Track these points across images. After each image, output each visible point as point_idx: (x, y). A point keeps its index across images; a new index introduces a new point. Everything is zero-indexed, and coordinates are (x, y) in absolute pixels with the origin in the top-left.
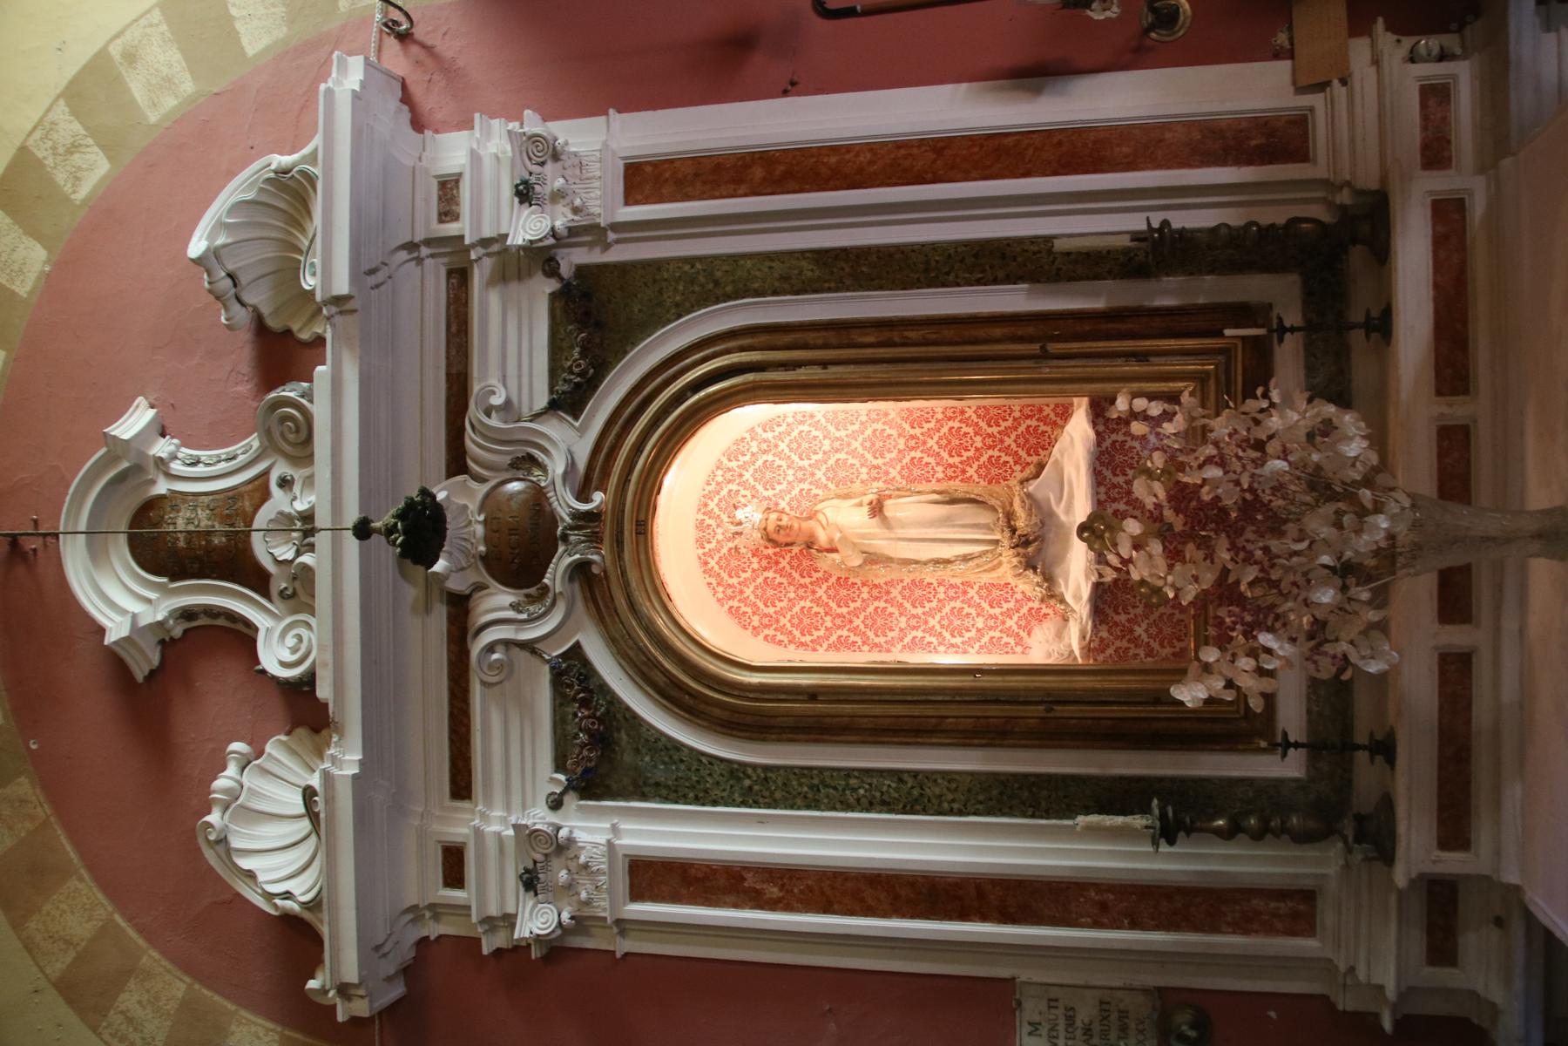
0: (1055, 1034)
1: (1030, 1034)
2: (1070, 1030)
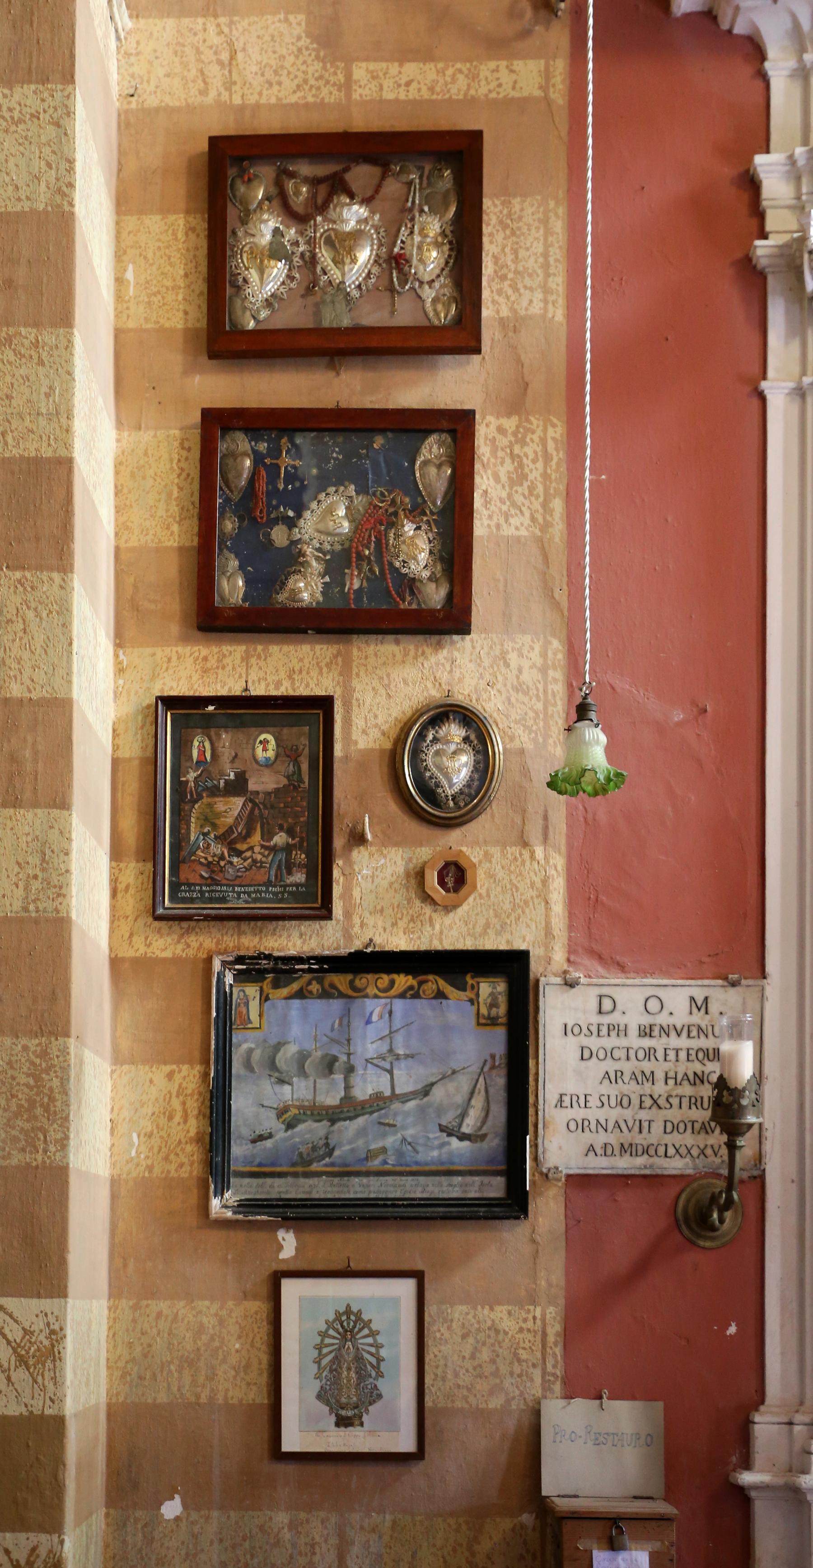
0: (694, 1033)
1: (692, 999)
2: (701, 1055)
